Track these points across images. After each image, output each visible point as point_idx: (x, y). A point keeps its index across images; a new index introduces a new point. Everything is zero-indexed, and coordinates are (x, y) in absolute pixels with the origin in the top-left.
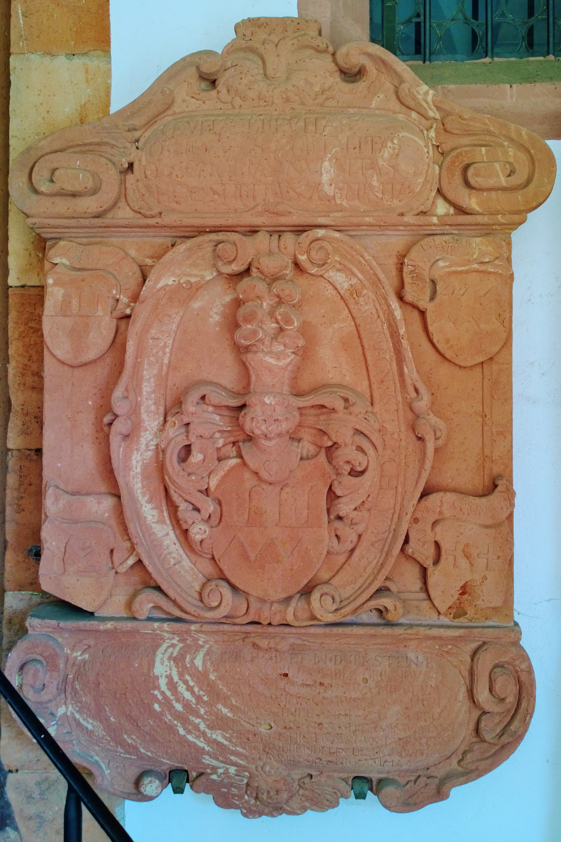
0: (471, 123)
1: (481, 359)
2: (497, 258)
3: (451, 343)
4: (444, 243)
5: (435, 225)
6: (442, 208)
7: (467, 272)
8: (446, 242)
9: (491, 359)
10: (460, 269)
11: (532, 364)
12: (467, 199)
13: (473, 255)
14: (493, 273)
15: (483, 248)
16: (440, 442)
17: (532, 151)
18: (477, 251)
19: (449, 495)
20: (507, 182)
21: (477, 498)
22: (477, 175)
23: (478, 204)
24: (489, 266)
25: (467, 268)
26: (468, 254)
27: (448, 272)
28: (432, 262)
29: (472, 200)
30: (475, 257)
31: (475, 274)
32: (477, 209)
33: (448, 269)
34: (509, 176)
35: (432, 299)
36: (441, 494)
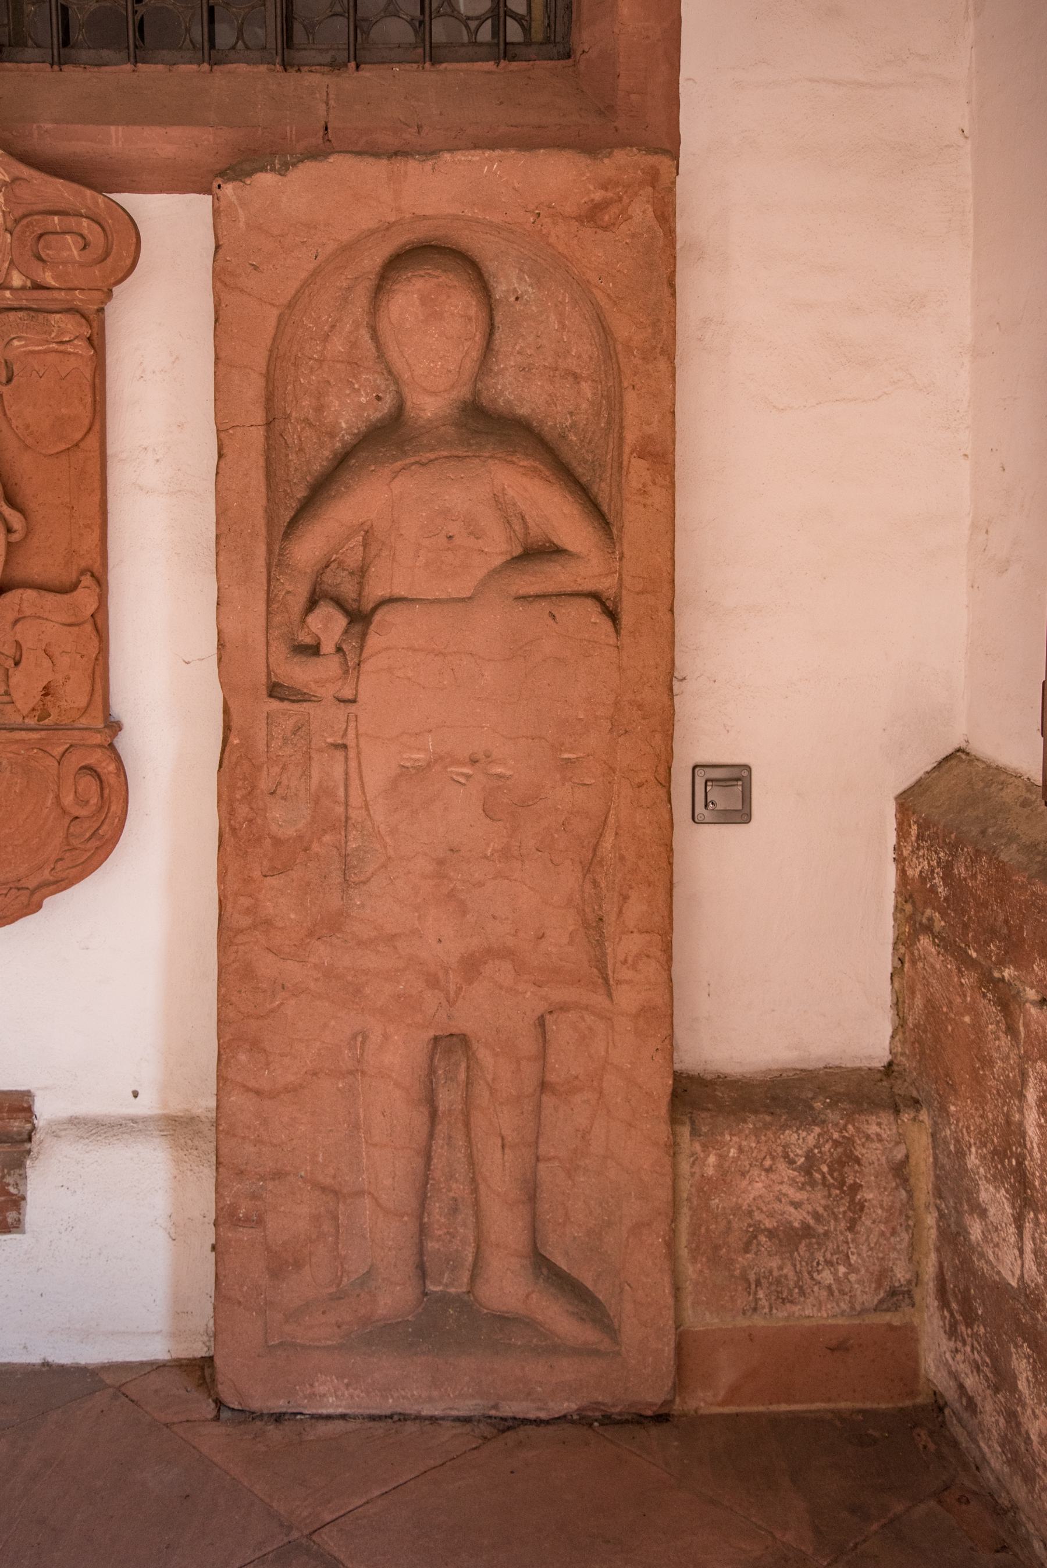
0: (42, 189)
1: (64, 446)
2: (76, 338)
3: (31, 429)
4: (19, 321)
5: (9, 299)
6: (17, 280)
7: (45, 352)
8: (20, 319)
9: (77, 445)
10: (37, 348)
11: (146, 449)
12: (41, 273)
13: (50, 334)
14: (73, 353)
15: (62, 325)
16: (15, 537)
17: (110, 221)
18: (55, 330)
19: (29, 591)
20: (80, 255)
21: (59, 595)
22: (47, 247)
23: (53, 278)
24: (69, 346)
25: (44, 347)
26: (45, 333)
27: (25, 352)
28: (6, 340)
29: (47, 274)
30: (53, 335)
31: (54, 354)
32: (53, 283)
33: (24, 349)
34: (84, 248)
35: (9, 380)
36: (20, 591)
